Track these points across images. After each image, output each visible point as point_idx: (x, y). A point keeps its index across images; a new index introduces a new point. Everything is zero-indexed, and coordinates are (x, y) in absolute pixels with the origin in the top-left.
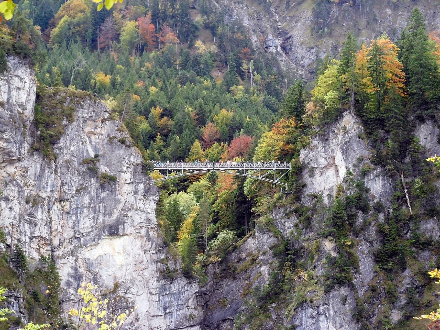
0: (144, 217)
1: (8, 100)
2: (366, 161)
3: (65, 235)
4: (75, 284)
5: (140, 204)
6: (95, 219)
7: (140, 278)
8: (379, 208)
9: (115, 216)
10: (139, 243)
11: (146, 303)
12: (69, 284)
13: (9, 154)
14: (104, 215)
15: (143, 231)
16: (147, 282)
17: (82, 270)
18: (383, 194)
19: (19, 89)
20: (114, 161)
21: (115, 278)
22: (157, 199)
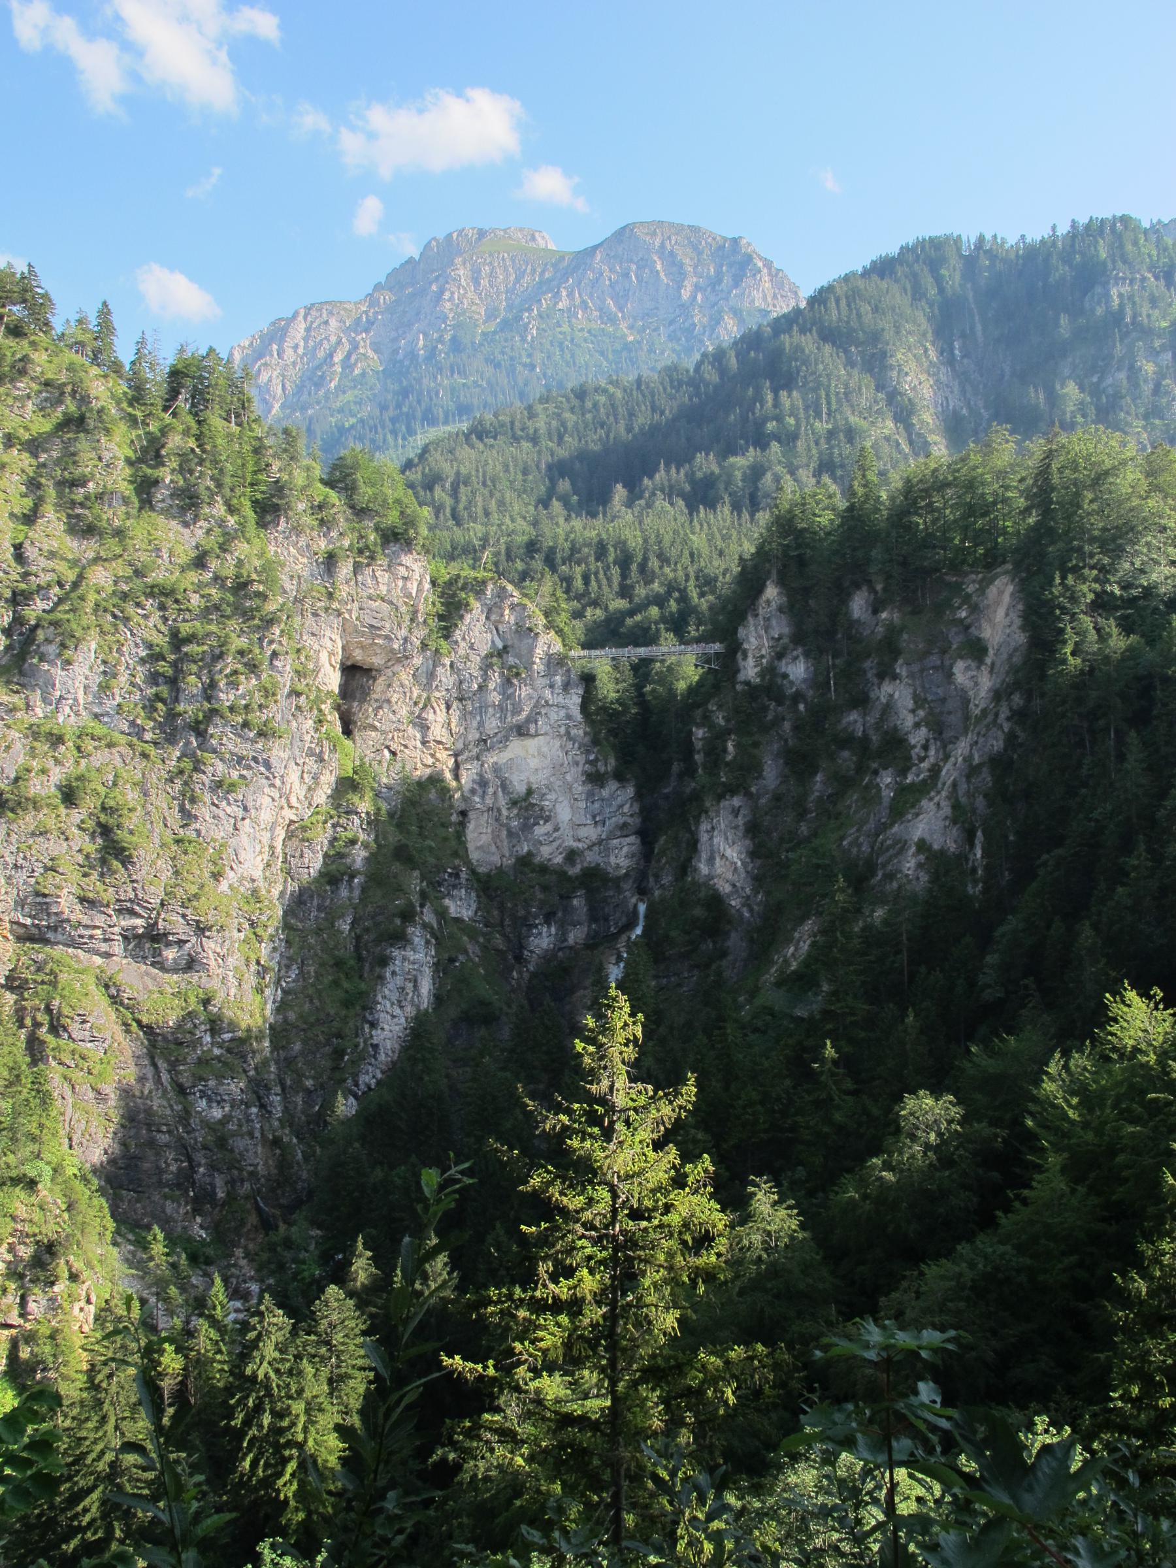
0: (562, 713)
1: (389, 591)
2: (786, 640)
3: (470, 738)
4: (480, 791)
5: (560, 699)
6: (503, 719)
7: (559, 783)
8: (798, 697)
9: (525, 714)
10: (557, 743)
11: (568, 810)
12: (473, 791)
13: (392, 651)
14: (513, 714)
15: (563, 730)
16: (570, 789)
17: (489, 776)
18: (805, 680)
19: (405, 579)
20: (524, 652)
21: (529, 783)
22: (581, 691)
